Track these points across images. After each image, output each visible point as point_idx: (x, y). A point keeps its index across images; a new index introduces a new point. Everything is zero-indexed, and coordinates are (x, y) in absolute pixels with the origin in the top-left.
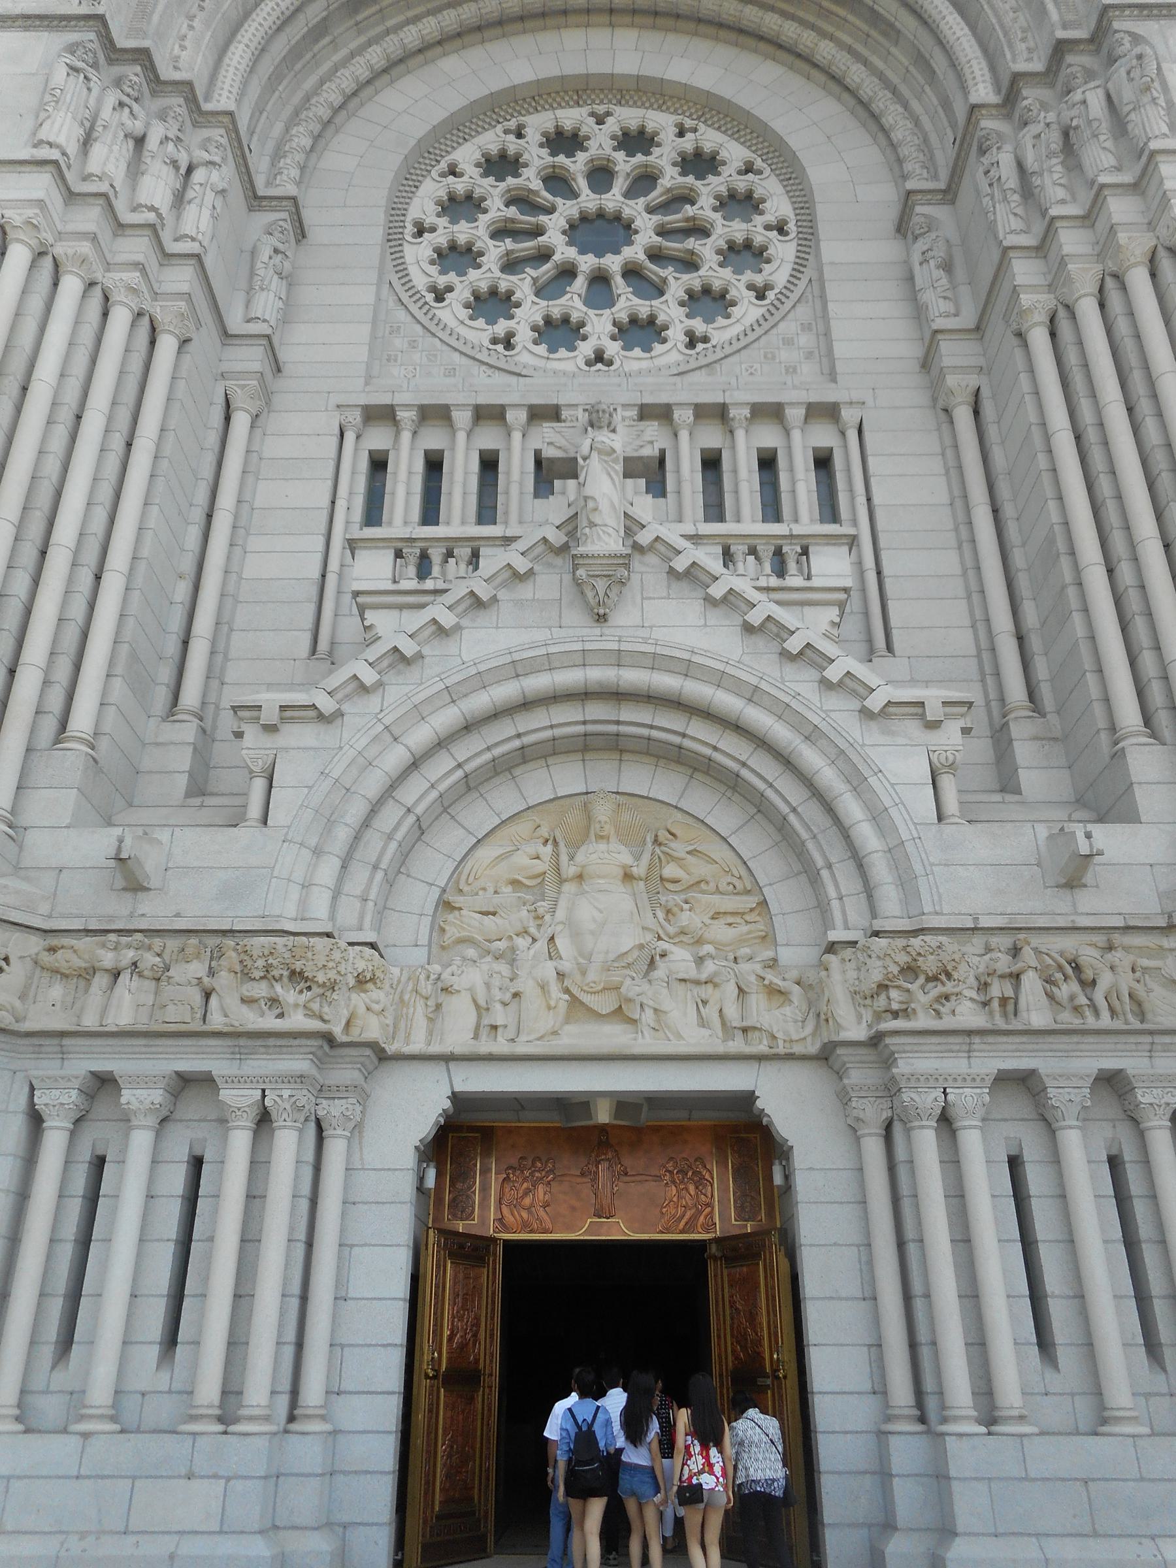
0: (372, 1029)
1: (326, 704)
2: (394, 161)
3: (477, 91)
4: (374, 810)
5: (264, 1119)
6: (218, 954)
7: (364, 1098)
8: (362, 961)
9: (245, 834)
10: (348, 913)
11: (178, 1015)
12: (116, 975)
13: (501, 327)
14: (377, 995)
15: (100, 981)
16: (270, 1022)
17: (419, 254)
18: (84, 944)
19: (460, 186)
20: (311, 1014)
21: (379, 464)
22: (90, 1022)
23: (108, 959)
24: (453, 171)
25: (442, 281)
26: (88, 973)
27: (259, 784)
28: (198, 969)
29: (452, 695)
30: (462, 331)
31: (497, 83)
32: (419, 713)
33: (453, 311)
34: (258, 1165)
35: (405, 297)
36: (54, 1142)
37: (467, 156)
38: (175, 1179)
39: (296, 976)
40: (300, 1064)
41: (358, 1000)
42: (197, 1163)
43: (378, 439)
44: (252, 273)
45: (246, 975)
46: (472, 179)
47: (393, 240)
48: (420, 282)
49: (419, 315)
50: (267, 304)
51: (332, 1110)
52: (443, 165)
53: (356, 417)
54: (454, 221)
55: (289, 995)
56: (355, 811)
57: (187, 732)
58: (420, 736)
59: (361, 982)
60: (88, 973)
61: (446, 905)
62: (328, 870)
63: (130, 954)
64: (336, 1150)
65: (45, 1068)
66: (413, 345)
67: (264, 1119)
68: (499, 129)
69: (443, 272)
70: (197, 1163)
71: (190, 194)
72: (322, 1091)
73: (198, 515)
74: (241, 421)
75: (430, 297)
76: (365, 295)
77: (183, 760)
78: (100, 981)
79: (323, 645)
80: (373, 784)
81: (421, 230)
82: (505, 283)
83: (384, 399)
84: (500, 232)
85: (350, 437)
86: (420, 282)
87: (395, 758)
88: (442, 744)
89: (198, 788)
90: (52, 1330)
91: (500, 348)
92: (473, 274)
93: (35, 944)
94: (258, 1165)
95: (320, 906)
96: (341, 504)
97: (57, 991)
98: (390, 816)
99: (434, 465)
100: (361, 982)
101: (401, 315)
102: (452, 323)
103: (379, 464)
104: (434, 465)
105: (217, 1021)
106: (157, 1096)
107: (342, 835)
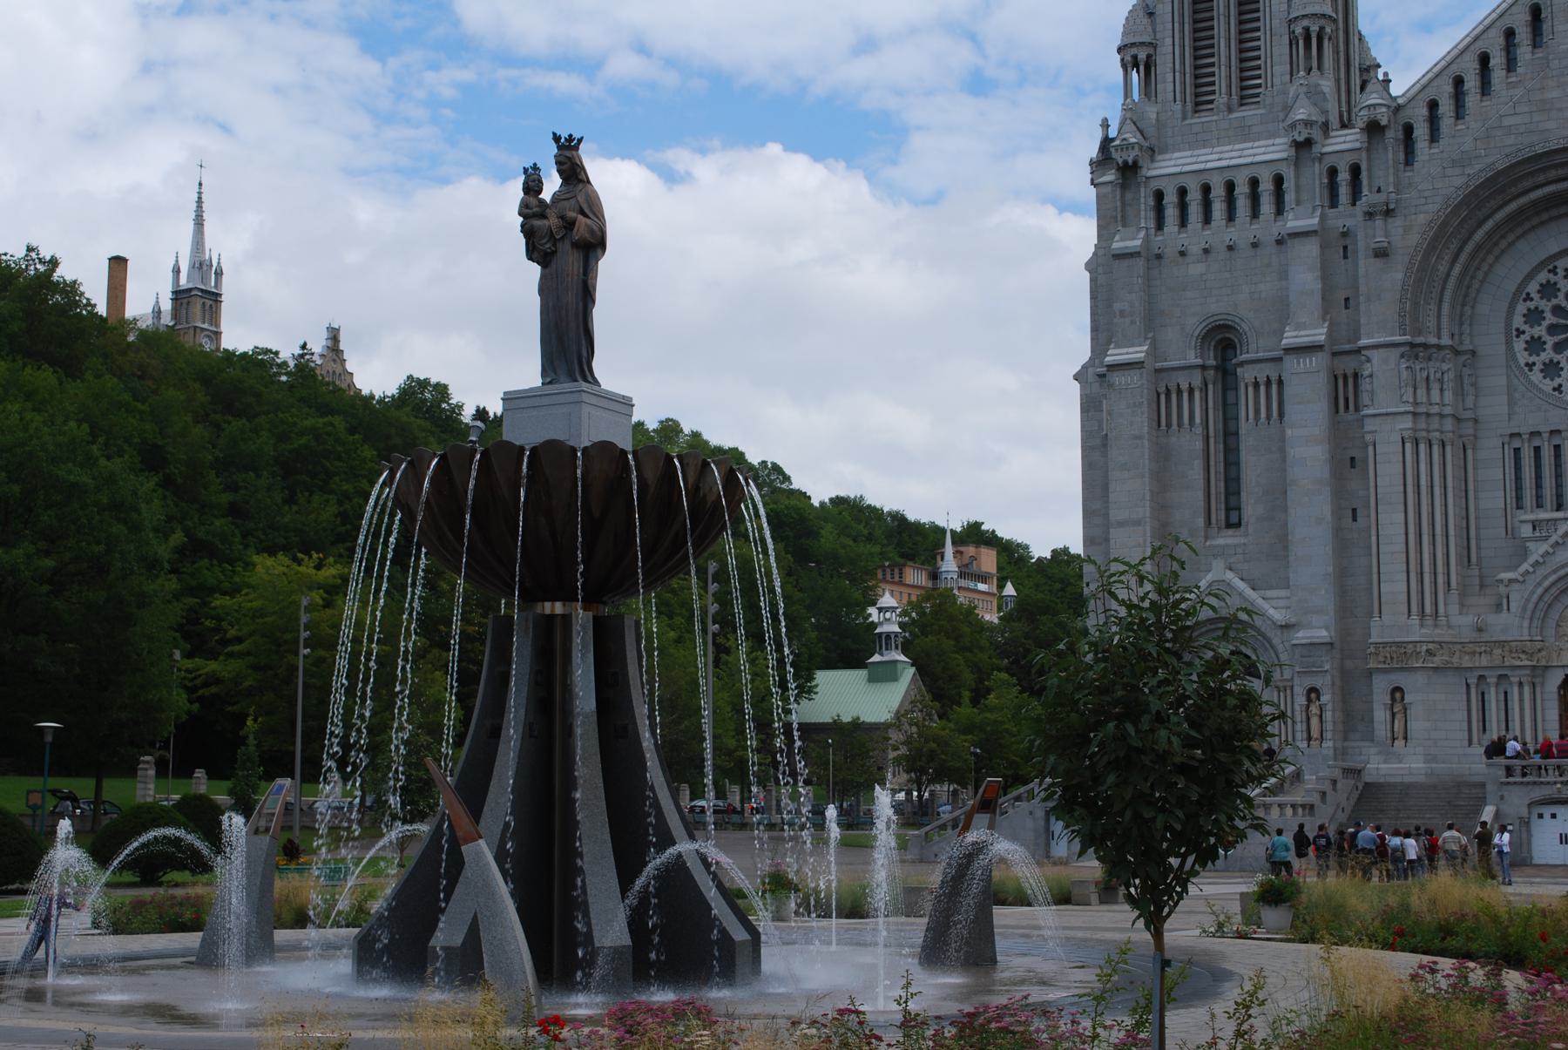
0: (1543, 663)
1: (1521, 579)
2: (1504, 306)
3: (1535, 262)
4: (1537, 604)
5: (1521, 684)
6: (1504, 646)
7: (1543, 677)
8: (1538, 645)
9: (1504, 613)
10: (1534, 631)
11: (1497, 663)
12: (1481, 653)
13: (1557, 381)
14: (1544, 653)
15: (1477, 655)
16: (1518, 663)
17: (1519, 345)
18: (1471, 645)
19: (1532, 305)
20: (1528, 660)
21: (1517, 450)
22: (1477, 665)
23: (1478, 650)
24: (1528, 298)
25: (1531, 360)
26: (1474, 653)
27: (1505, 601)
28: (1500, 651)
29: (1555, 571)
30: (1541, 386)
31: (1543, 256)
32: (1546, 577)
33: (1536, 376)
34: (1521, 694)
35: (1517, 373)
36: (1473, 691)
37: (1533, 288)
38: (1502, 697)
39: (1524, 652)
40: (1528, 672)
41: (1540, 655)
42: (1506, 693)
43: (1516, 444)
44: (1463, 389)
45: (1511, 651)
46: (1538, 302)
47: (1509, 343)
48: (1522, 362)
49: (1524, 381)
50: (1470, 401)
51: (1537, 680)
52: (1524, 296)
53: (1507, 439)
54: (1532, 327)
55: (1523, 656)
56: (1531, 606)
57: (1476, 572)
58: (1547, 583)
59: (1540, 651)
60: (1474, 653)
61: (1558, 625)
62: (1526, 623)
63: (1483, 649)
64: (1538, 690)
65: (1468, 675)
66: (1523, 396)
67: (1521, 684)
68: (1546, 270)
69: (1530, 355)
70: (1506, 693)
71: (1445, 387)
72: (1533, 676)
73: (1464, 494)
74: (1470, 452)
75: (1526, 369)
76: (1503, 381)
77: (1477, 581)
78: (1477, 655)
79: (1509, 532)
80: (1535, 598)
81: (1520, 333)
82: (1557, 358)
83: (1516, 431)
84: (1552, 329)
85: (1506, 447)
86: (1522, 362)
87: (1540, 591)
88: (1553, 584)
89: (1482, 586)
90: (1481, 728)
91: (1556, 393)
92: (1543, 354)
93: (1459, 646)
94: (1521, 694)
95: (1526, 631)
96: (1507, 476)
97: (1467, 657)
98: (1541, 604)
99: (1537, 449)
100: (1540, 651)
101: (1516, 381)
102: (1537, 382)
103: (1517, 450)
104: (1537, 449)
105: (1507, 664)
106: (1495, 680)
107: (1529, 613)
